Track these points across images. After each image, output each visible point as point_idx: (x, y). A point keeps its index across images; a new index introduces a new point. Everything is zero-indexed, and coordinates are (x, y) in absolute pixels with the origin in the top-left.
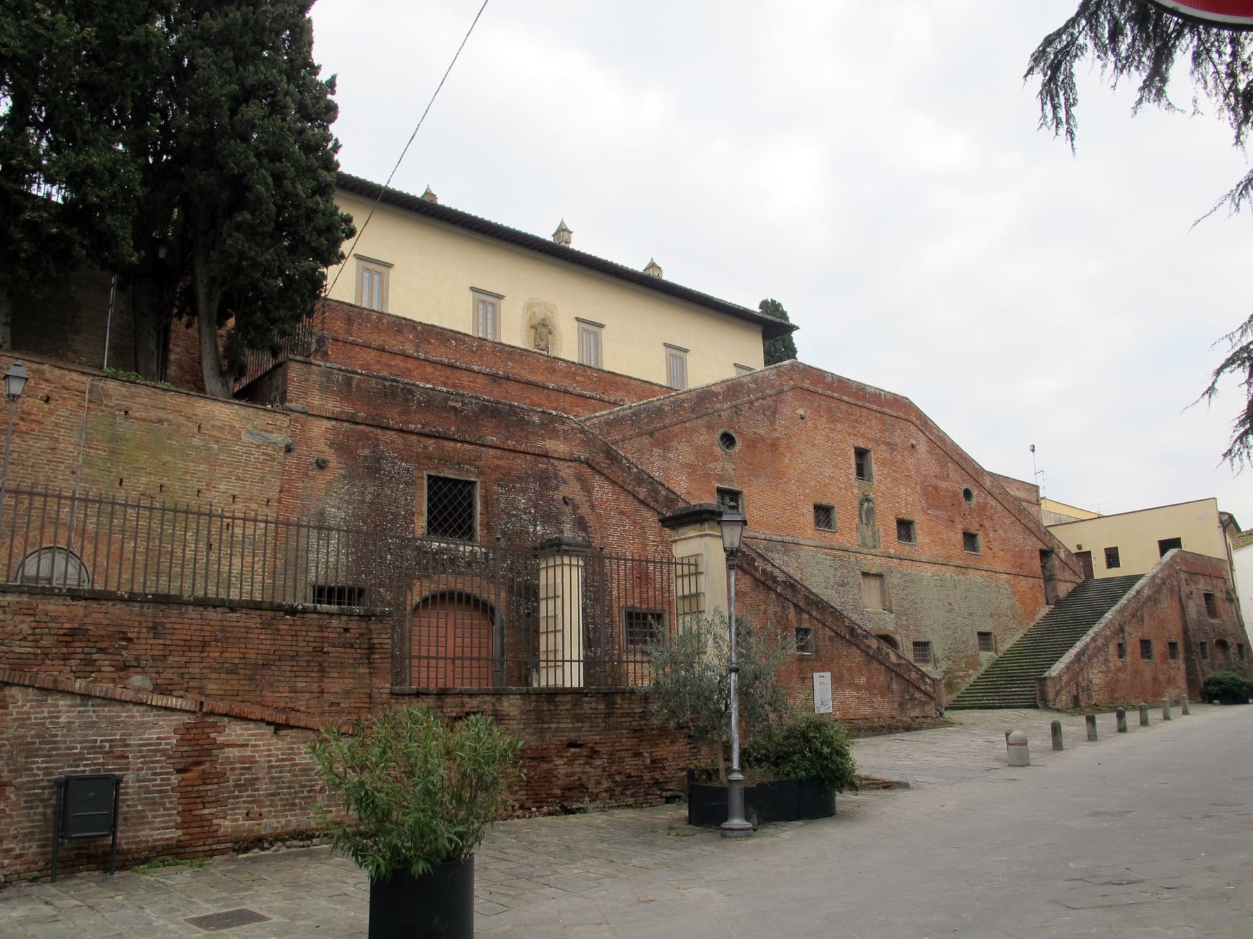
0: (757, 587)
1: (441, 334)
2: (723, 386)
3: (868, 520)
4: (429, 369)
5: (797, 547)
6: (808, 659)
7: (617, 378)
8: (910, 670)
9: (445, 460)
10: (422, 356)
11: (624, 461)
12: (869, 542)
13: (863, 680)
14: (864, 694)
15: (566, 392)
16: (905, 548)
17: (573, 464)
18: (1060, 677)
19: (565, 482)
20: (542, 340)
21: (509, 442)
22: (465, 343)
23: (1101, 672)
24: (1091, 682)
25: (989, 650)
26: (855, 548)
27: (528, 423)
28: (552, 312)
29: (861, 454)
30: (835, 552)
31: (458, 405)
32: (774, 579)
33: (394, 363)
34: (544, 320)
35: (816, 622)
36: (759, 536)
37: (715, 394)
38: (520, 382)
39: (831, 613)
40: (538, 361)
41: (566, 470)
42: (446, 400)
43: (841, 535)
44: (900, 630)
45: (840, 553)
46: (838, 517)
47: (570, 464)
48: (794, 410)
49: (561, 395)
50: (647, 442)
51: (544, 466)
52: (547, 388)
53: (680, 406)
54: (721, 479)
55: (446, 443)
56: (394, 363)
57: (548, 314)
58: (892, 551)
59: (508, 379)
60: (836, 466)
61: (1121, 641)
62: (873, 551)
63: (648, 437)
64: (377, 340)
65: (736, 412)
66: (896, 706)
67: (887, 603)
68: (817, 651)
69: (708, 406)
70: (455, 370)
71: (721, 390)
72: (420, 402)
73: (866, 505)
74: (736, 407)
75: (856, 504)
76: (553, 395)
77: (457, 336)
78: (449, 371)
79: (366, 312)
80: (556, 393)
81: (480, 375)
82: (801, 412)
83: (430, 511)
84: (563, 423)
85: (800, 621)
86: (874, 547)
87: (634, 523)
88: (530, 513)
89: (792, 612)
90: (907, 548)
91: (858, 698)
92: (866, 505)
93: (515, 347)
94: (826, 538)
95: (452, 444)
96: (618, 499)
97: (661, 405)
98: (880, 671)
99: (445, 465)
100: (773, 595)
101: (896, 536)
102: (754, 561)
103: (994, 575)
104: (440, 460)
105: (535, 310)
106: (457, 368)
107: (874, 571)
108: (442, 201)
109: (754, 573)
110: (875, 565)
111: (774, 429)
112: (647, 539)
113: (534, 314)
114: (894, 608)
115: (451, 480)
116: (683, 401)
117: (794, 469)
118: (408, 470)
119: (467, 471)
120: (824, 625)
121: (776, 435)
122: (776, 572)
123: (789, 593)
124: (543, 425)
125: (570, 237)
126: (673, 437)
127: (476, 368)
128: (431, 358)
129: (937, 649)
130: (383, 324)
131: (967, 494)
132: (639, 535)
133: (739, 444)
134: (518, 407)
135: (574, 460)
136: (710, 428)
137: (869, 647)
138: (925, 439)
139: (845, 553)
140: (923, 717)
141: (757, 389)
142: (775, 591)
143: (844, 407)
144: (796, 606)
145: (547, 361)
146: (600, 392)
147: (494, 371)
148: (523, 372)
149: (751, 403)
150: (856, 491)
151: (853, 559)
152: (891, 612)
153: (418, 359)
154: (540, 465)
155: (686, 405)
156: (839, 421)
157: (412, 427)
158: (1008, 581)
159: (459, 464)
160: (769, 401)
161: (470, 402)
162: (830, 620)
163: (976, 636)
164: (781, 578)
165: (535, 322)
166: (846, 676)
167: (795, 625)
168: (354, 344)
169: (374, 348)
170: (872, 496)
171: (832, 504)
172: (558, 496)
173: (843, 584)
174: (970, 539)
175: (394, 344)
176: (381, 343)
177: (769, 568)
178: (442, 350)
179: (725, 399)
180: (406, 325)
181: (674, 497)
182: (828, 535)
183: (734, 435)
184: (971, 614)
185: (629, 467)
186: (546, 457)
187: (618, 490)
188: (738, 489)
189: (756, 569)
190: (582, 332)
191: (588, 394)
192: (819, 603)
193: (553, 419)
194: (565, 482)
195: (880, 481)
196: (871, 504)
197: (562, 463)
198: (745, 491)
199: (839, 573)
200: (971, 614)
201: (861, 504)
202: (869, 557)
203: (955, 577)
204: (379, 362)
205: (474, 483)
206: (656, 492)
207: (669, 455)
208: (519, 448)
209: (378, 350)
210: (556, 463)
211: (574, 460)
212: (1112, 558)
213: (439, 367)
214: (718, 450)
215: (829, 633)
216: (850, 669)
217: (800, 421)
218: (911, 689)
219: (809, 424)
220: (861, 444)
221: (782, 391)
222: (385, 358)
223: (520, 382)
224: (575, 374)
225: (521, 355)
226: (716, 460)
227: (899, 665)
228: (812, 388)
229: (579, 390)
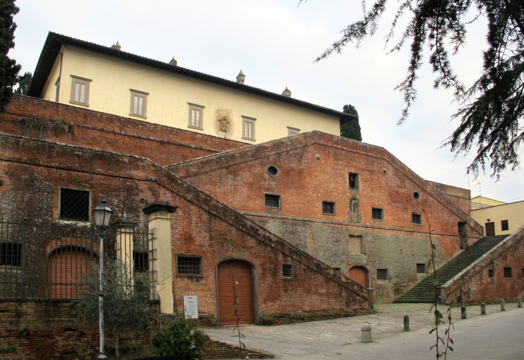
0: (259, 244)
1: (134, 122)
2: (271, 143)
3: (354, 209)
4: (127, 139)
5: (311, 223)
6: (289, 280)
7: (230, 142)
8: (354, 285)
9: (71, 181)
10: (123, 133)
11: (179, 181)
12: (355, 220)
13: (324, 291)
14: (324, 298)
15: (201, 149)
16: (377, 222)
17: (147, 182)
18: (449, 287)
19: (142, 191)
20: (223, 127)
21: (110, 172)
22: (146, 126)
23: (478, 284)
24: (470, 289)
25: (423, 272)
26: (347, 222)
27: (121, 162)
28: (229, 114)
29: (353, 177)
30: (334, 225)
31: (80, 153)
32: (270, 240)
33: (108, 137)
34: (225, 117)
35: (295, 262)
36: (288, 217)
37: (267, 148)
38: (176, 145)
39: (305, 257)
40: (186, 134)
41: (143, 185)
42: (73, 151)
43: (338, 216)
44: (369, 263)
45: (337, 226)
46: (337, 207)
47: (146, 182)
48: (314, 155)
49: (199, 151)
50: (225, 172)
51: (130, 184)
52: (191, 147)
53: (245, 154)
54: (268, 189)
55: (73, 173)
56: (108, 137)
57: (227, 114)
58: (368, 224)
59: (169, 143)
60: (337, 182)
61: (491, 268)
62: (357, 224)
63: (226, 169)
64: (100, 126)
65: (278, 157)
66: (344, 303)
67: (363, 250)
68: (295, 276)
69: (262, 153)
70: (141, 140)
71: (270, 146)
72: (58, 152)
73: (353, 201)
74: (278, 154)
75: (348, 201)
76: (194, 151)
77: (142, 123)
78: (138, 140)
79: (94, 113)
80: (195, 150)
81: (154, 142)
82: (318, 155)
83: (62, 206)
84: (142, 162)
85: (286, 261)
86: (358, 222)
87: (184, 212)
88: (120, 207)
89: (281, 257)
90: (378, 223)
91: (320, 300)
92: (353, 201)
93: (173, 128)
94: (330, 218)
95: (76, 173)
96: (175, 200)
97: (234, 154)
98: (335, 286)
99: (71, 183)
100: (269, 248)
101: (371, 217)
102: (258, 231)
104: (68, 181)
105: (221, 112)
106: (142, 139)
107: (356, 234)
108: (180, 64)
109: (257, 237)
110: (356, 230)
111: (301, 165)
112: (192, 220)
113: (220, 114)
114: (367, 253)
115: (75, 191)
116: (247, 151)
117: (312, 184)
118: (50, 186)
119: (84, 186)
120: (300, 263)
121: (301, 167)
122: (272, 237)
123: (279, 247)
124: (130, 163)
125: (244, 78)
126: (240, 169)
127: (152, 138)
128: (128, 134)
129: (391, 272)
130: (103, 118)
131: (416, 195)
132: (187, 218)
133: (279, 172)
134: (116, 154)
135: (148, 180)
136: (262, 164)
137: (329, 274)
139: (340, 226)
140: (361, 309)
141: (292, 144)
142: (271, 246)
144: (283, 254)
145: (191, 135)
146: (220, 149)
147: (162, 139)
148: (178, 140)
149: (288, 152)
150: (348, 195)
151: (344, 228)
152: (365, 254)
153: (121, 134)
154: (128, 183)
155: (249, 153)
156: (340, 160)
157: (53, 164)
158: (438, 238)
159: (79, 182)
160: (299, 150)
161: (88, 152)
162: (304, 261)
163: (416, 266)
164: (274, 239)
165: (220, 118)
166: (313, 289)
167: (282, 263)
168: (88, 128)
169: (98, 130)
170: (358, 197)
171: (334, 201)
172: (138, 198)
173: (337, 241)
174: (416, 218)
175: (109, 128)
176: (102, 127)
177: (267, 234)
178: (135, 130)
179: (272, 150)
180: (115, 119)
181: (209, 198)
182: (330, 217)
183: (276, 168)
184: (413, 255)
185: (182, 184)
186: (132, 179)
187: (174, 195)
188: (278, 194)
189: (259, 235)
190: (244, 122)
191: (213, 150)
192: (298, 251)
193: (137, 160)
194: (142, 191)
195: (363, 190)
196: (357, 201)
197: (141, 182)
198: (282, 196)
199: (335, 236)
200: (413, 255)
201: (351, 201)
202: (354, 227)
203: (406, 237)
204: (101, 136)
205: (88, 192)
206: (199, 196)
207: (237, 178)
208: (115, 174)
209: (100, 130)
210: (137, 182)
211: (148, 180)
212: (505, 225)
213: (132, 138)
214: (266, 176)
215: (303, 267)
216: (316, 286)
217: (317, 160)
218: (354, 295)
219: (322, 162)
220: (353, 171)
221: (307, 146)
222: (104, 134)
223: (176, 145)
224: (206, 140)
225: (177, 132)
226: (265, 180)
227: (347, 283)
228: (325, 144)
229: (208, 148)
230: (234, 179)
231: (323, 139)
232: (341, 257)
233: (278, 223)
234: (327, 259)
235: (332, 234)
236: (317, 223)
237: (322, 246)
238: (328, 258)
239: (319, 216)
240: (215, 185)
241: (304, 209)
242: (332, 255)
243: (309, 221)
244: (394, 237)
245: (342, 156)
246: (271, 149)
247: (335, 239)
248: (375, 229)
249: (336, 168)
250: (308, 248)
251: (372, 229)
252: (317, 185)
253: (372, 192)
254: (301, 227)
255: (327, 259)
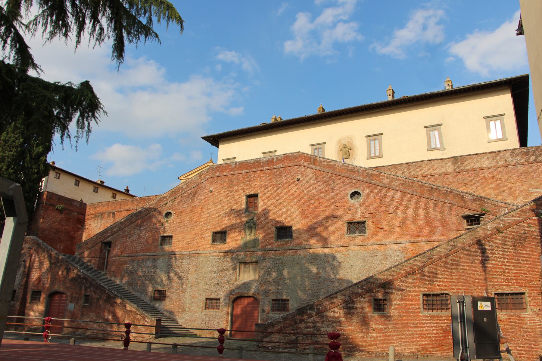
2: (170, 192)
16: (283, 242)
37: (165, 197)
82: (211, 189)
103: (382, 247)
123: (84, 281)
138: (312, 171)
141: (188, 187)
143: (241, 177)
217: (210, 194)
230: (140, 230)
231: (218, 171)
232: (223, 287)
233: (167, 259)
234: (207, 289)
235: (217, 264)
236: (204, 254)
237: (204, 277)
238: (208, 288)
239: (208, 247)
240: (127, 237)
241: (193, 243)
242: (212, 285)
243: (195, 254)
244: (308, 257)
245: (239, 180)
246: (169, 197)
247: (220, 268)
248: (277, 252)
249: (231, 196)
250: (190, 279)
251: (273, 252)
252: (208, 218)
253: (277, 208)
254: (187, 260)
255: (207, 289)
